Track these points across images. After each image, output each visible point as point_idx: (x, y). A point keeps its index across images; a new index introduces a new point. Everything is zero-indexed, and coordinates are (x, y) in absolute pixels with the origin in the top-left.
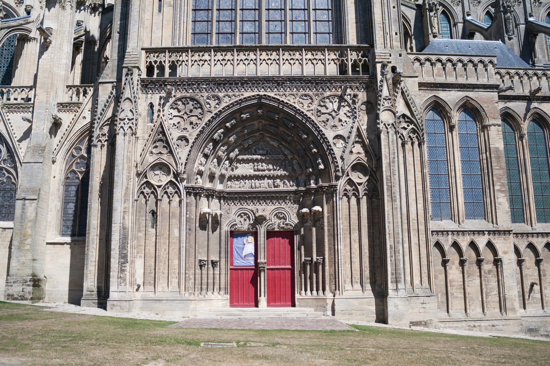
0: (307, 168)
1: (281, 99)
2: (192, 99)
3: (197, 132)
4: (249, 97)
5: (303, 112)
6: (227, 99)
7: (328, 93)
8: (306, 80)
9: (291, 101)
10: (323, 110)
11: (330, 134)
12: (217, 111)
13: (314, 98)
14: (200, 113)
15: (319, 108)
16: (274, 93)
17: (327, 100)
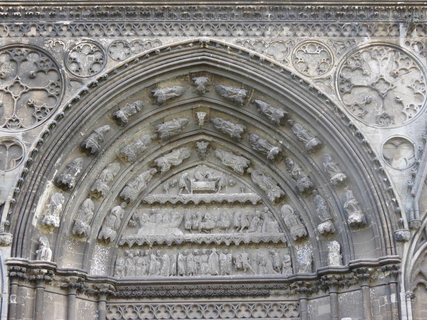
0: (319, 222)
1: (252, 52)
2: (35, 49)
3: (45, 128)
4: (173, 47)
5: (306, 84)
6: (120, 53)
7: (367, 41)
8: (311, 10)
9: (277, 56)
10: (356, 79)
11: (376, 137)
12: (94, 79)
13: (332, 51)
14: (53, 84)
15: (347, 75)
16: (234, 39)
17: (365, 56)
